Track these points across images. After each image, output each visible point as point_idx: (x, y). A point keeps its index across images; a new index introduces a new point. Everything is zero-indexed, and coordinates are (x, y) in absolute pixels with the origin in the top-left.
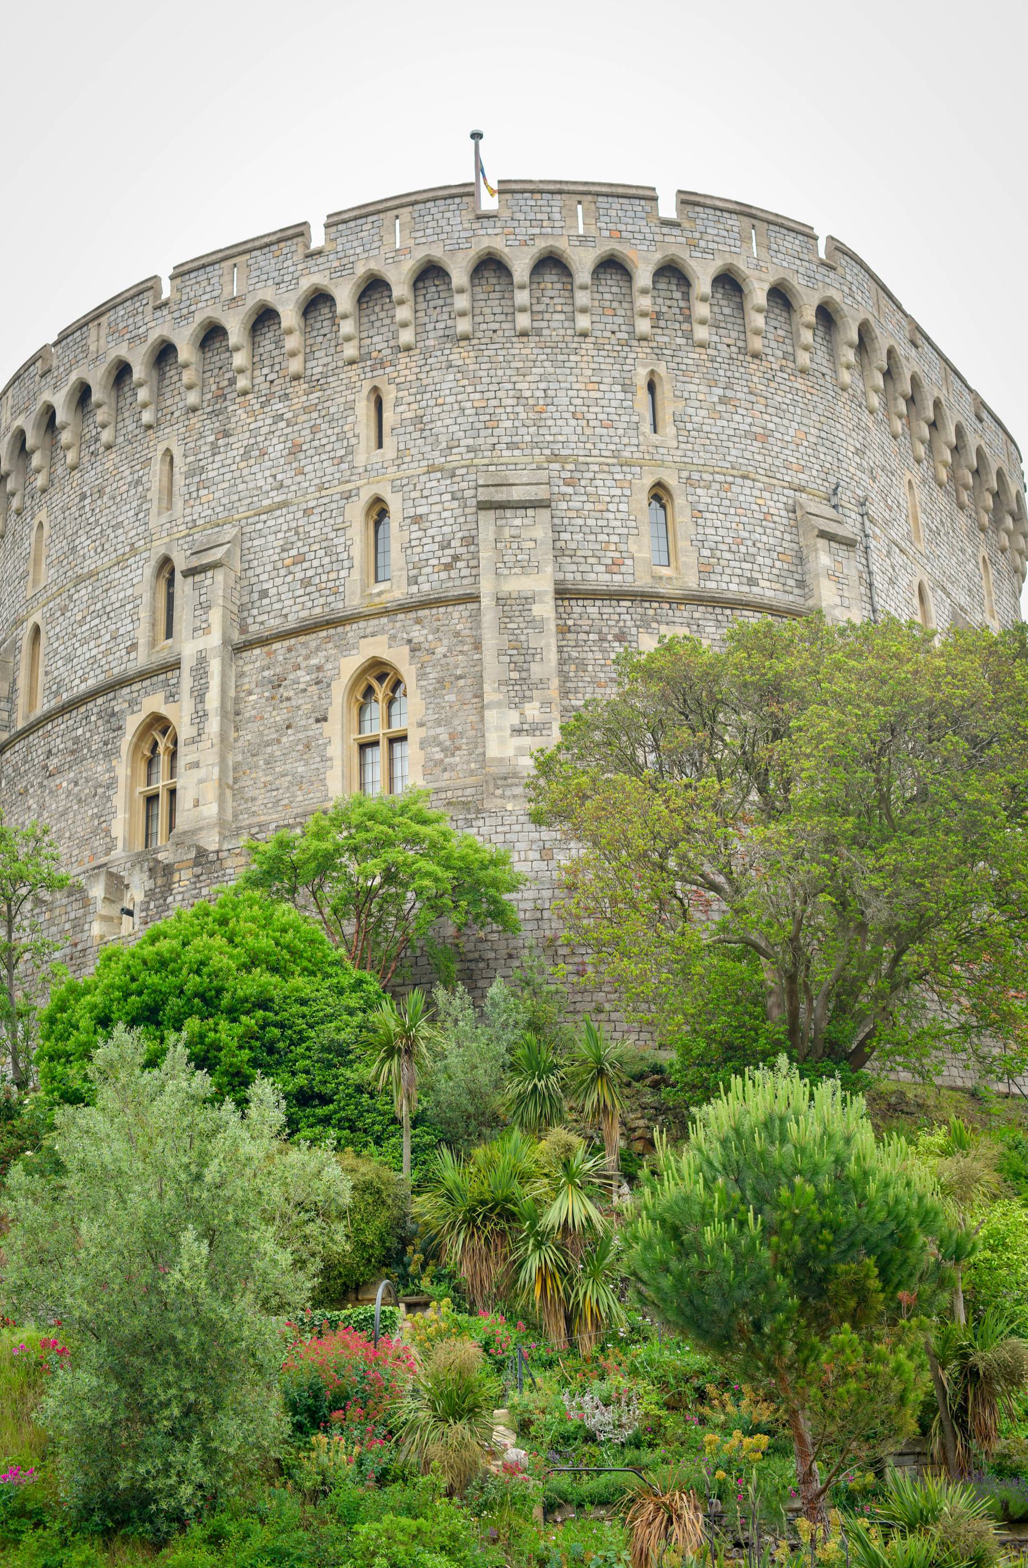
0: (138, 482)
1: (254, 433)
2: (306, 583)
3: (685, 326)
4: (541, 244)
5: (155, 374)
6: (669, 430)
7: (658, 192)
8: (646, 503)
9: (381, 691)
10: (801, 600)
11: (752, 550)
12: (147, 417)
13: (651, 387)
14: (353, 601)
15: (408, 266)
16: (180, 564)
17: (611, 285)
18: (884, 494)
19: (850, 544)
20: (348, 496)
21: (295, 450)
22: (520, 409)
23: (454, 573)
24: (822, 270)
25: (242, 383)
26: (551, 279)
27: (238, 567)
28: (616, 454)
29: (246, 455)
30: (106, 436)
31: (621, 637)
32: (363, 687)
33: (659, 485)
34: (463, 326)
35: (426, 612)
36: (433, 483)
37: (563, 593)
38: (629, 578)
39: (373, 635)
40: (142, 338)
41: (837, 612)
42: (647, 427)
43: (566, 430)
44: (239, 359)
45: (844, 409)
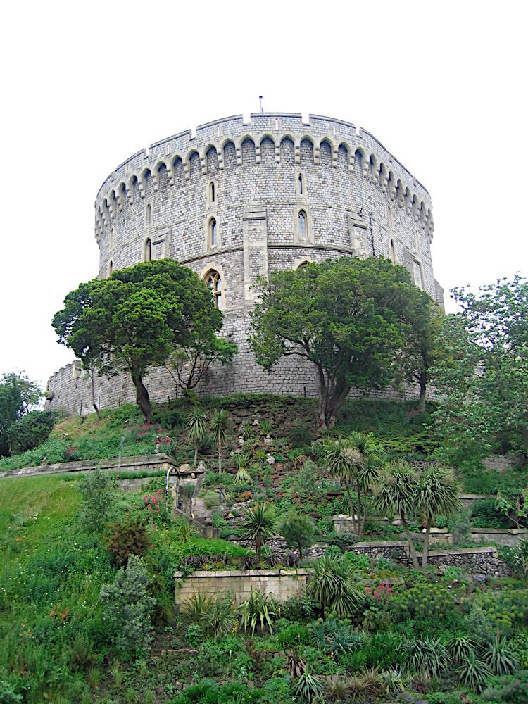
0: (140, 215)
1: (175, 198)
2: (191, 245)
3: (312, 159)
4: (264, 133)
5: (145, 180)
6: (305, 193)
7: (302, 115)
8: (298, 217)
9: (214, 280)
10: (348, 247)
11: (333, 231)
12: (143, 194)
13: (300, 179)
14: (205, 252)
15: (222, 142)
16: (152, 242)
17: (287, 146)
18: (379, 212)
19: (365, 228)
20: (203, 217)
21: (187, 203)
22: (257, 188)
23: (236, 241)
24: (358, 138)
25: (171, 182)
26: (267, 144)
27: (170, 241)
28: (288, 201)
29: (172, 206)
30: (131, 200)
31: (288, 261)
32: (208, 278)
33: (302, 210)
34: (239, 161)
35: (227, 254)
36: (230, 212)
37: (269, 247)
38: (292, 241)
39: (211, 261)
40: (140, 169)
41: (360, 250)
42: (298, 192)
43: (272, 194)
44: (170, 174)
45: (365, 183)
